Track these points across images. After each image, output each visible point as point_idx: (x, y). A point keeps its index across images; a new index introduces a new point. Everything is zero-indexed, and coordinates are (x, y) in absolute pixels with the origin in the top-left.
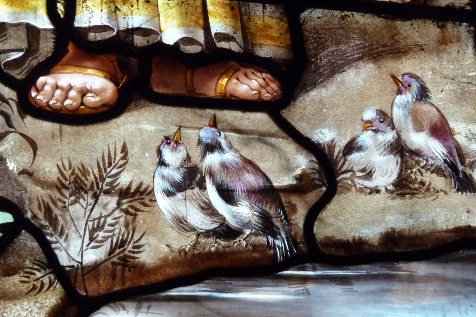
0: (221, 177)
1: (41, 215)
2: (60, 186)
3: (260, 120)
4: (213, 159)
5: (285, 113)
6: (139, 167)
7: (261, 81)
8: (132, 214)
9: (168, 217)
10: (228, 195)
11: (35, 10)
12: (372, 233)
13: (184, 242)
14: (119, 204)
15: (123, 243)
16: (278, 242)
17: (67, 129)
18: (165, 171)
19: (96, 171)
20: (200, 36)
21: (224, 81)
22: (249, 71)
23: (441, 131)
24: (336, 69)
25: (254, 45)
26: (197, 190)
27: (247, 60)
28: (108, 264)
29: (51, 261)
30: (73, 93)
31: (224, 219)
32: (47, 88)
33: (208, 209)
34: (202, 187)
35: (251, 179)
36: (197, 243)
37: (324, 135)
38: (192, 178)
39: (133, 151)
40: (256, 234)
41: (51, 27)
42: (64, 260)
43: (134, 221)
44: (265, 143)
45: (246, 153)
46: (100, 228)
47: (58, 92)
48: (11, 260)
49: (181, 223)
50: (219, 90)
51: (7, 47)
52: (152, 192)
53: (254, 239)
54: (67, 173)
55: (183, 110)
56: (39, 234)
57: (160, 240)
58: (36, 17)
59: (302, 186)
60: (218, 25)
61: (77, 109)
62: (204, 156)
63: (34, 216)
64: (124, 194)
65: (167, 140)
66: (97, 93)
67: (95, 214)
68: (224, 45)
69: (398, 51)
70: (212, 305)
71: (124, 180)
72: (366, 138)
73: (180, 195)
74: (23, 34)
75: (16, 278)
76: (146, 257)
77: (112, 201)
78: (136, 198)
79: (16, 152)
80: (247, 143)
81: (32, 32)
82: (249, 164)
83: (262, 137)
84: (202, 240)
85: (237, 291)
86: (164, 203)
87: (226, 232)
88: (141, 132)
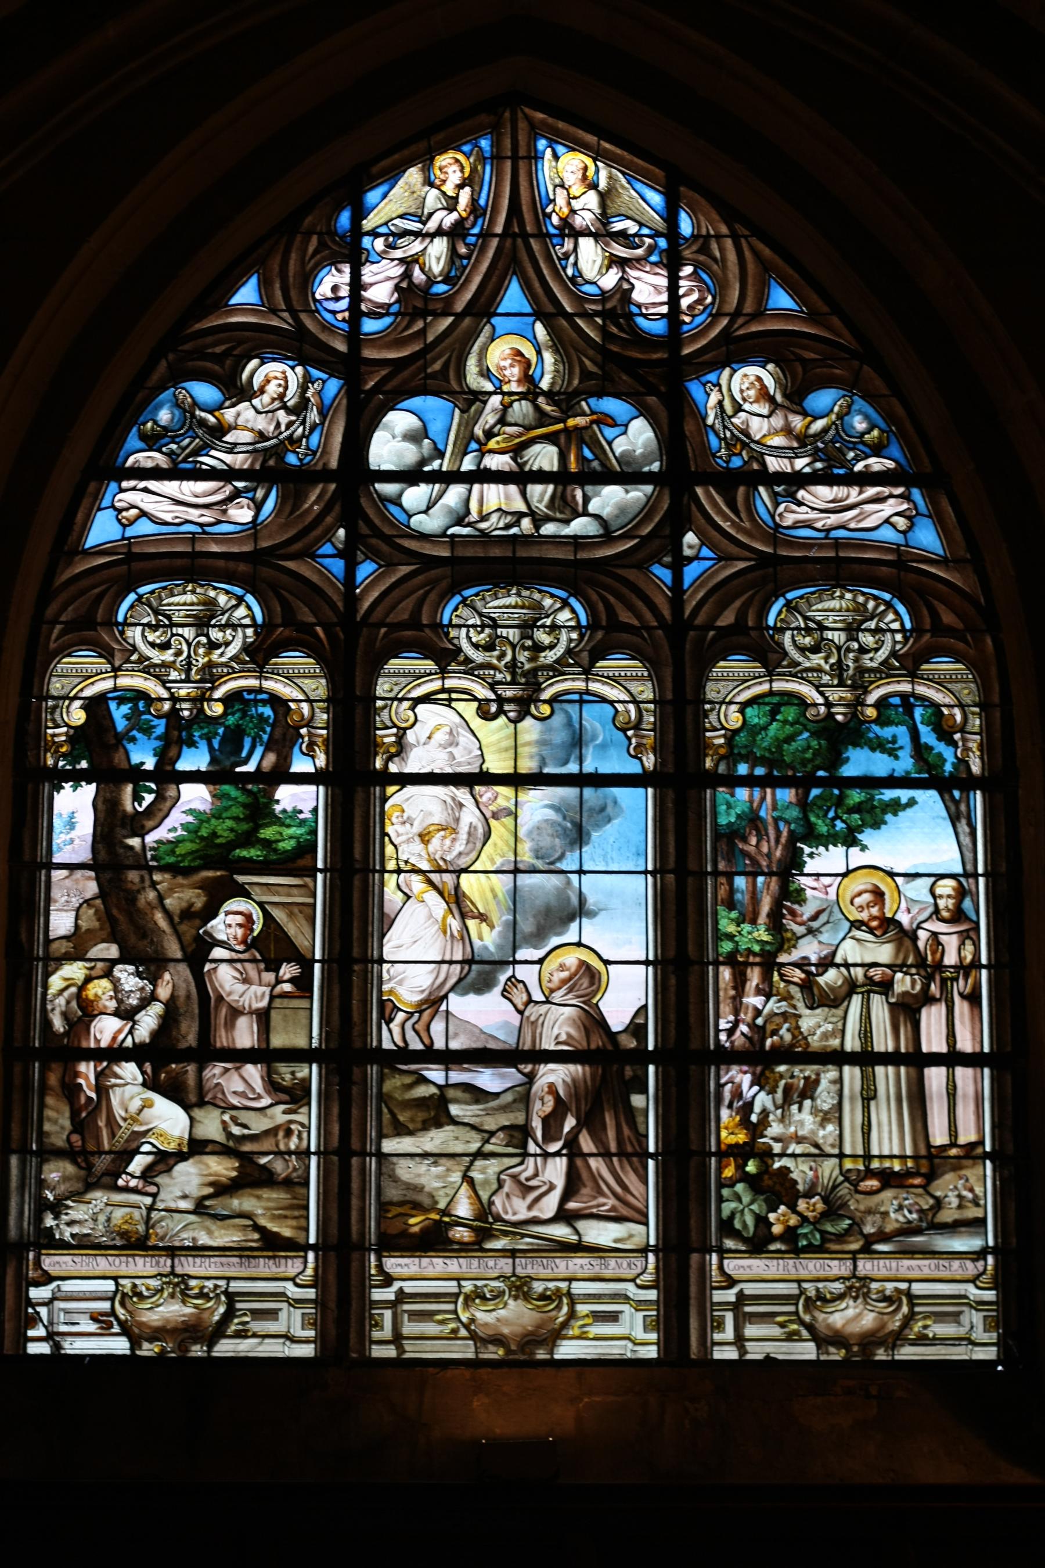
3: (920, 1191)
4: (907, 1202)
10: (910, 1212)
12: (949, 1220)
13: (897, 1225)
23: (971, 1190)
24: (943, 1174)
27: (917, 1174)
29: (861, 1233)
37: (938, 1194)
38: (901, 1208)
49: (897, 1221)
56: (858, 1225)
59: (932, 1208)
69: (960, 1168)
71: (882, 1209)
72: (950, 1194)
78: (886, 1214)
81: (859, 1171)
82: (917, 1203)
83: (920, 1195)
86: (892, 1215)
87: (909, 1222)
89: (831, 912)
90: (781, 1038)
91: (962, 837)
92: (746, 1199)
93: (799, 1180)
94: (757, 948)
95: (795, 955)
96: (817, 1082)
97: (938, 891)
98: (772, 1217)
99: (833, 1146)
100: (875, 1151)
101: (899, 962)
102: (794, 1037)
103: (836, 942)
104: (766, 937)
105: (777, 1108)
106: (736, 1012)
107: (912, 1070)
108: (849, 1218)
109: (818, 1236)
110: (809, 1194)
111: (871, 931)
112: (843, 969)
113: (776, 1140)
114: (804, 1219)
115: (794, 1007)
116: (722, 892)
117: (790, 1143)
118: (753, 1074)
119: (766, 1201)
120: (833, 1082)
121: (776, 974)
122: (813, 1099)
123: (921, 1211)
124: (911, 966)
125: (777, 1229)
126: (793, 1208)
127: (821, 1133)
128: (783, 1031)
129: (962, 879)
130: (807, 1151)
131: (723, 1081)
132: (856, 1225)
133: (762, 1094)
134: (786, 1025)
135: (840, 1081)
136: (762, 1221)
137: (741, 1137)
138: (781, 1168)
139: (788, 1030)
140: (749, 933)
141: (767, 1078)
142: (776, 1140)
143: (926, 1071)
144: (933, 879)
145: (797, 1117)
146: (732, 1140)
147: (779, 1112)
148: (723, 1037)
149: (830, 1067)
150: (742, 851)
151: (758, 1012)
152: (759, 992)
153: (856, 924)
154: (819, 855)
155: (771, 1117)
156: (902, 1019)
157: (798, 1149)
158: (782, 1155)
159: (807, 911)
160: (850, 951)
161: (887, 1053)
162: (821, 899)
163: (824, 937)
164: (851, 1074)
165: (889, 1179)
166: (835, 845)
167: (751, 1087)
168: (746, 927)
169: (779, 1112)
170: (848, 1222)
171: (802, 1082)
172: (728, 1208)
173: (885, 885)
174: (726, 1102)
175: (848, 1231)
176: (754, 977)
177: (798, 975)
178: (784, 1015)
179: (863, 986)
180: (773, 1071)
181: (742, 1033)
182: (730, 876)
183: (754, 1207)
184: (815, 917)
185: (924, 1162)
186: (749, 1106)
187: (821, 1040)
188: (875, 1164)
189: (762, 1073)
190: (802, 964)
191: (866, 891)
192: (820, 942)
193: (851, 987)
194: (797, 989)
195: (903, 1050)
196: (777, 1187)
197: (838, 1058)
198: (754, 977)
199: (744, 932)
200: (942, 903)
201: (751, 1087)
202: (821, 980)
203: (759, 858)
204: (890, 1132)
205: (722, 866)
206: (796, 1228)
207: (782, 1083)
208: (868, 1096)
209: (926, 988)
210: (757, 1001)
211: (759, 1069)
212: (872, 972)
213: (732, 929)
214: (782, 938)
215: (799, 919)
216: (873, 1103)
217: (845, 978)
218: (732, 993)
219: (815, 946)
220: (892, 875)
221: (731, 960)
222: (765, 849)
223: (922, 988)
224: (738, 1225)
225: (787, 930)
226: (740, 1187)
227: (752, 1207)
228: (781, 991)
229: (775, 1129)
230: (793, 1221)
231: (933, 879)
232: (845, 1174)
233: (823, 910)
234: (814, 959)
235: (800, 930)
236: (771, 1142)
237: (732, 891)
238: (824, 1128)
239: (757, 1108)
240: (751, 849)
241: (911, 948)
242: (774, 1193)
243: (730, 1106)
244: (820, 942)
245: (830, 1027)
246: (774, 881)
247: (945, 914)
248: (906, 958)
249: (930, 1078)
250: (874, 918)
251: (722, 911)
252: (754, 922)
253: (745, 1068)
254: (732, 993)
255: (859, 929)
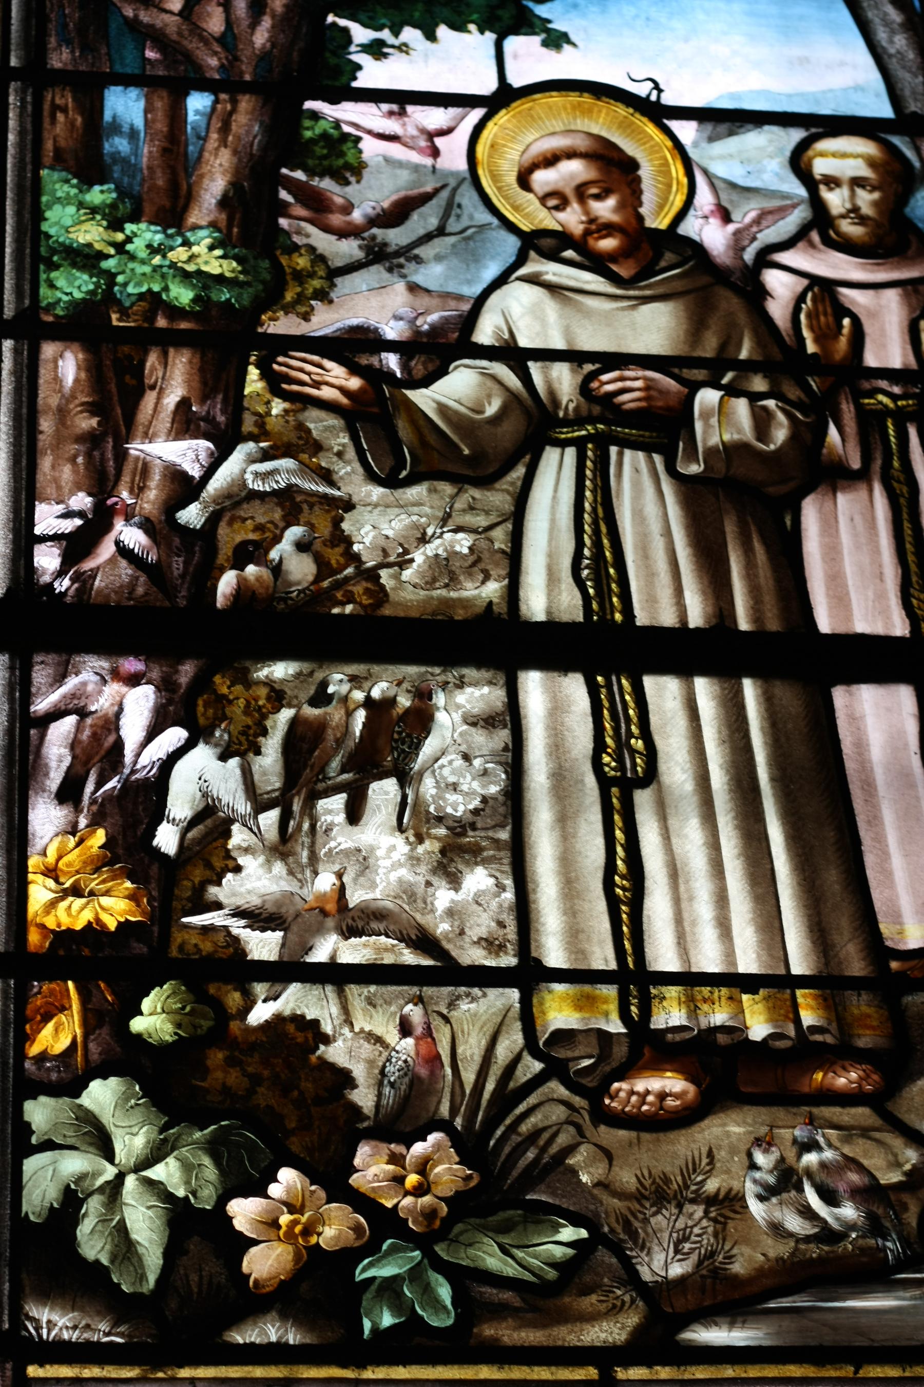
0: (821, 1177)
1: (619, 1229)
2: (639, 1197)
3: (861, 1114)
4: (811, 1159)
5: (890, 1106)
6: (728, 1172)
7: (861, 1073)
8: (721, 1224)
9: (762, 1223)
10: (830, 1197)
11: (606, 1014)
13: (779, 1249)
14: (706, 1212)
15: (712, 1254)
16: (889, 1244)
17: (646, 1136)
18: (758, 1175)
19: (679, 1179)
20: (791, 1031)
21: (819, 1076)
22: (847, 1064)
25: (851, 1036)
26: (793, 1193)
27: (842, 1053)
28: (697, 1277)
29: (632, 1278)
30: (650, 1098)
31: (826, 1222)
32: (622, 1094)
33: (807, 1213)
34: (801, 1190)
35: (854, 1177)
36: (796, 1249)
38: (787, 1181)
39: (721, 1155)
40: (863, 1237)
41: (624, 1031)
42: (646, 1275)
43: (724, 1229)
44: (870, 1138)
45: (847, 1150)
46: (686, 1239)
47: (634, 1099)
48: (587, 1278)
49: (777, 1229)
50: (814, 1085)
51: (577, 1053)
52: (743, 1199)
53: (861, 1242)
54: (647, 1183)
55: (774, 1109)
56: (617, 1249)
57: (754, 1249)
58: (608, 1021)
60: (808, 1018)
61: (656, 1114)
62: (799, 1156)
63: (612, 1230)
64: (711, 1201)
65: (758, 1142)
66: (677, 1096)
67: (680, 1224)
68: (818, 1038)
70: (816, 1316)
71: (712, 1186)
73: (774, 1200)
74: (594, 1041)
75: (594, 1298)
76: (737, 1268)
77: (699, 1211)
78: (729, 1204)
79: (590, 1163)
80: (847, 1140)
81: (602, 1035)
82: (851, 1163)
83: (865, 1132)
84: (802, 1247)
85: (845, 1300)
86: (756, 1208)
88: (728, 1134)
89: (450, 207)
90: (277, 569)
91: (882, 35)
92: (131, 1142)
93: (359, 1071)
94: (183, 295)
95: (325, 321)
96: (421, 720)
97: (821, 167)
98: (244, 1212)
99: (492, 945)
100: (663, 956)
101: (709, 348)
102: (324, 568)
103: (476, 290)
104: (215, 264)
105: (260, 807)
106: (101, 484)
107: (785, 693)
108: (576, 1220)
109: (445, 1293)
110: (398, 1125)
111: (596, 263)
112: (501, 370)
113: (260, 918)
114: (382, 1224)
115: (327, 476)
116: (61, 129)
117: (320, 930)
118: (165, 686)
119: (213, 1148)
120: (488, 722)
121: (253, 373)
122: (404, 778)
123: (871, 1193)
124: (749, 367)
125: (264, 1263)
126: (333, 1178)
127: (443, 897)
128: (283, 549)
129: (896, 140)
130: (388, 959)
131: (41, 705)
132: (608, 1249)
133: (202, 757)
134: (294, 532)
135: (511, 716)
136: (196, 1229)
137: (115, 907)
138: (278, 1020)
139: (301, 546)
140: (153, 250)
141: (222, 701)
142: (260, 918)
143: (840, 695)
144: (797, 135)
145: (344, 838)
146: (75, 915)
147: (269, 819)
148: (47, 560)
149: (470, 673)
150: (133, 25)
151: (184, 488)
152: (185, 424)
153: (537, 243)
154: (404, 48)
155: (239, 836)
156: (730, 529)
157: (354, 952)
158: (282, 972)
159: (368, 197)
160: (522, 313)
161: (682, 632)
162: (416, 168)
163: (431, 274)
164: (556, 704)
165: (725, 1071)
166: (458, 26)
167: (153, 733)
168: (144, 235)
169: (269, 819)
170: (568, 1233)
171: (361, 716)
172: (44, 1178)
173: (641, 143)
174: (55, 779)
175: (573, 1270)
176: (173, 381)
177: (336, 380)
178: (289, 503)
179: (578, 421)
180: (244, 679)
181: (123, 551)
182: (89, 89)
183: (166, 1172)
184: (398, 213)
185: (860, 1005)
186: (151, 794)
187: (431, 583)
188: (670, 1014)
189: (201, 683)
190: (354, 346)
191: (571, 154)
192: (413, 288)
193: (534, 426)
194: (334, 421)
195: (744, 625)
196: (264, 1097)
197: (503, 643)
198: (173, 381)
199: (138, 246)
200: (836, 200)
201: (153, 733)
202: (424, 399)
203: (192, 44)
204: (722, 899)
205: (60, 58)
206: (348, 1257)
207: (286, 715)
208: (624, 775)
209: (807, 438)
210: (187, 454)
211: (187, 671)
212: (609, 382)
213: (91, 234)
214: (277, 267)
215: (336, 219)
216: (643, 799)
217: (511, 397)
218: (88, 423)
219: (397, 296)
220: (657, 112)
221: (82, 325)
222: (215, 23)
223: (794, 437)
224: (92, 1243)
225: (296, 248)
226: (101, 1095)
227: (157, 1172)
228: (272, 424)
229: (255, 879)
230: (336, 1228)
231: (797, 135)
232: (553, 1050)
233: (425, 199)
234: (392, 331)
235: (347, 249)
236: (237, 927)
237: (95, 127)
238: (455, 882)
239: (181, 802)
240: (170, 23)
241: (742, 317)
242: (248, 1117)
243: (69, 793)
244: (413, 288)
245: (463, 543)
246: (246, 118)
247: (849, 228)
248: (729, 342)
249: (856, 720)
250: (608, 229)
251: (58, 185)
252: (173, 216)
253: (132, 665)
254: (88, 423)
255: (553, 256)
